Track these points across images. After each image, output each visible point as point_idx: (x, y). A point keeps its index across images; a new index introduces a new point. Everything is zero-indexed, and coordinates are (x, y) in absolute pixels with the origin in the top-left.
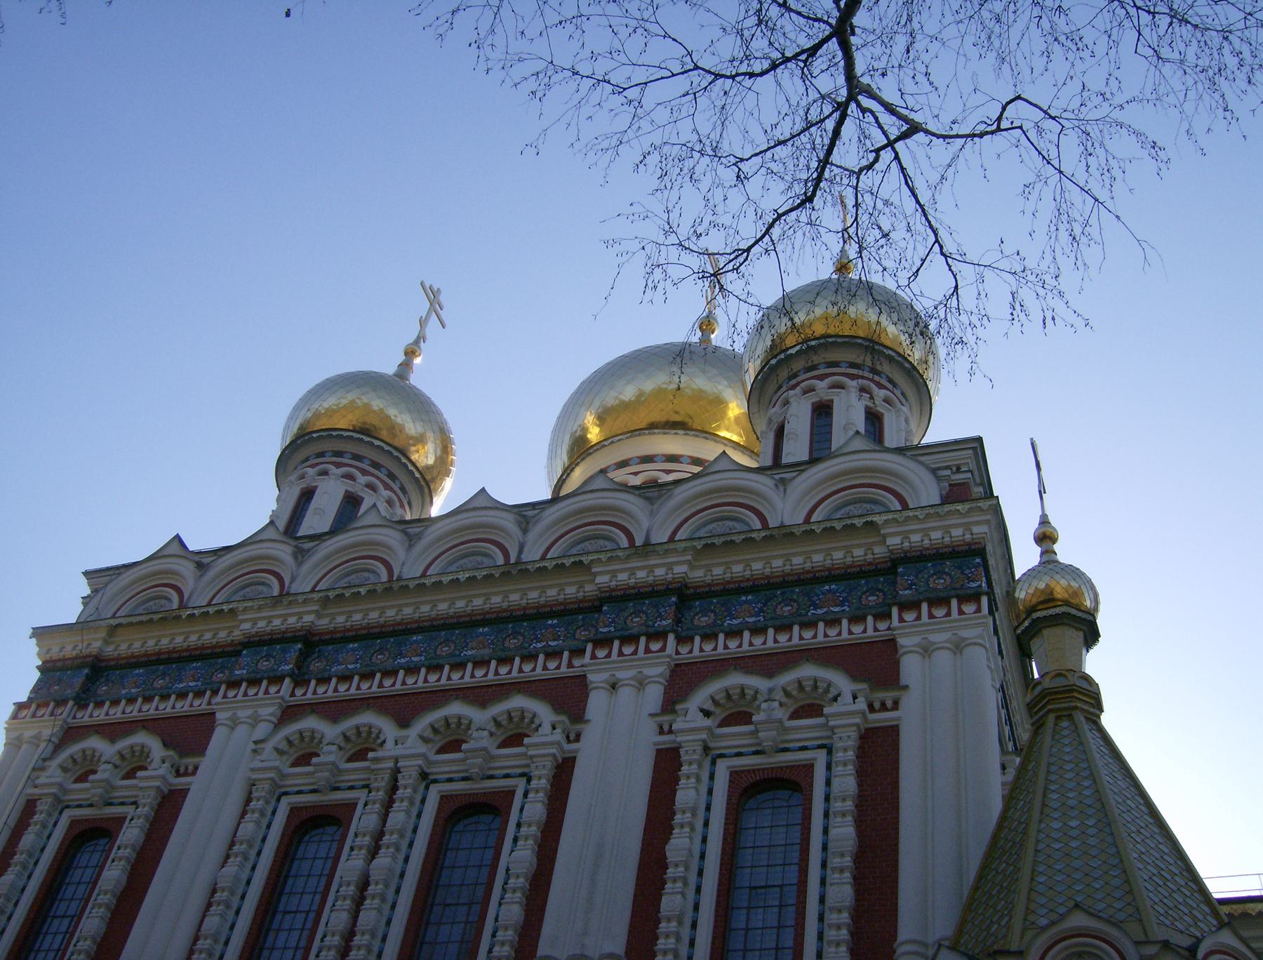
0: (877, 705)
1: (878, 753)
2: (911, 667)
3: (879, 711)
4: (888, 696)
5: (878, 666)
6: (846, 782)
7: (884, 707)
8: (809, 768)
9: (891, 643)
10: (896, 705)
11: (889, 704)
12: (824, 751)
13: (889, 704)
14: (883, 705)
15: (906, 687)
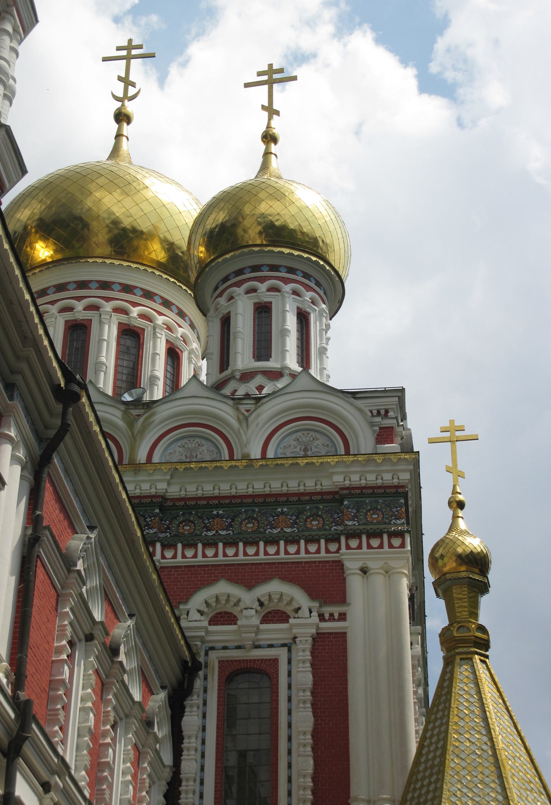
0: (327, 616)
1: (331, 654)
2: (355, 585)
3: (329, 620)
4: (336, 610)
5: (327, 586)
6: (304, 677)
7: (332, 618)
8: (275, 662)
9: (339, 565)
10: (343, 617)
11: (336, 616)
12: (286, 649)
13: (336, 616)
14: (331, 615)
15: (350, 604)
